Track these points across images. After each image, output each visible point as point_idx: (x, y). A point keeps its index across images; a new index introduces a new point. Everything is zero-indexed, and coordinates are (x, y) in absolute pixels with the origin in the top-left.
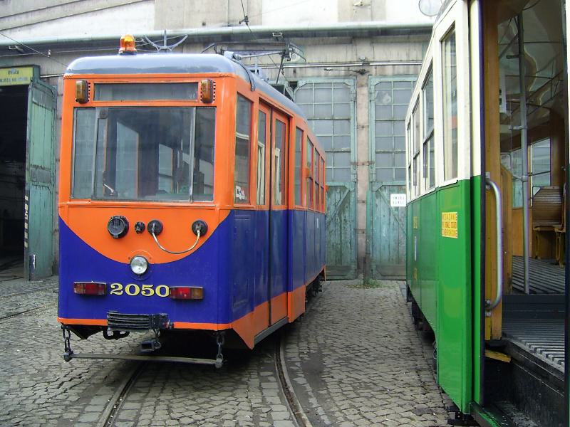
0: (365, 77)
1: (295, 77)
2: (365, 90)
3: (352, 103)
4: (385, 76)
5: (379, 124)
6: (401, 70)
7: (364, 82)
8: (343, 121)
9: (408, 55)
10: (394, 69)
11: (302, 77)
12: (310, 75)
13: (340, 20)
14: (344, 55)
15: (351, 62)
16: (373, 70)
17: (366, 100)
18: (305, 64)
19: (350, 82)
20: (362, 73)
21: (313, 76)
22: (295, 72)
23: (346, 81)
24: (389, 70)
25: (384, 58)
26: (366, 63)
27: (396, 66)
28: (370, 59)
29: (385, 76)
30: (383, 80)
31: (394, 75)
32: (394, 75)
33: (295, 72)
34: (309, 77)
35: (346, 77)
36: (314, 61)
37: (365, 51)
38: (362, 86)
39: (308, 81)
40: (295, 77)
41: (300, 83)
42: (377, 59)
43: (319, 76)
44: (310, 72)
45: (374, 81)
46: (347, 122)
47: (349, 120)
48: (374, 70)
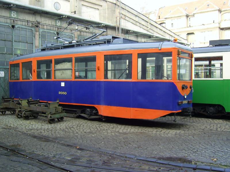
0: (38, 28)
1: (14, 23)
2: (38, 33)
3: (34, 37)
4: (44, 29)
5: (11, 53)
6: (49, 28)
7: (38, 30)
8: (30, 44)
9: (51, 23)
10: (47, 27)
11: (17, 24)
12: (19, 24)
13: (30, 4)
14: (31, 18)
15: (34, 22)
16: (40, 26)
17: (38, 37)
18: (18, 19)
19: (33, 29)
20: (37, 26)
21: (20, 25)
22: (14, 21)
23: (32, 29)
24: (45, 27)
25: (44, 22)
26: (39, 23)
27: (47, 26)
28: (40, 21)
29: (44, 29)
30: (44, 30)
31: (47, 29)
32: (47, 29)
33: (14, 21)
34: (19, 24)
35: (32, 27)
36: (21, 19)
37: (38, 19)
38: (37, 31)
39: (19, 26)
40: (14, 23)
41: (16, 26)
42: (42, 22)
43: (22, 25)
44: (19, 23)
45: (41, 30)
46: (31, 45)
47: (33, 44)
48: (41, 26)
